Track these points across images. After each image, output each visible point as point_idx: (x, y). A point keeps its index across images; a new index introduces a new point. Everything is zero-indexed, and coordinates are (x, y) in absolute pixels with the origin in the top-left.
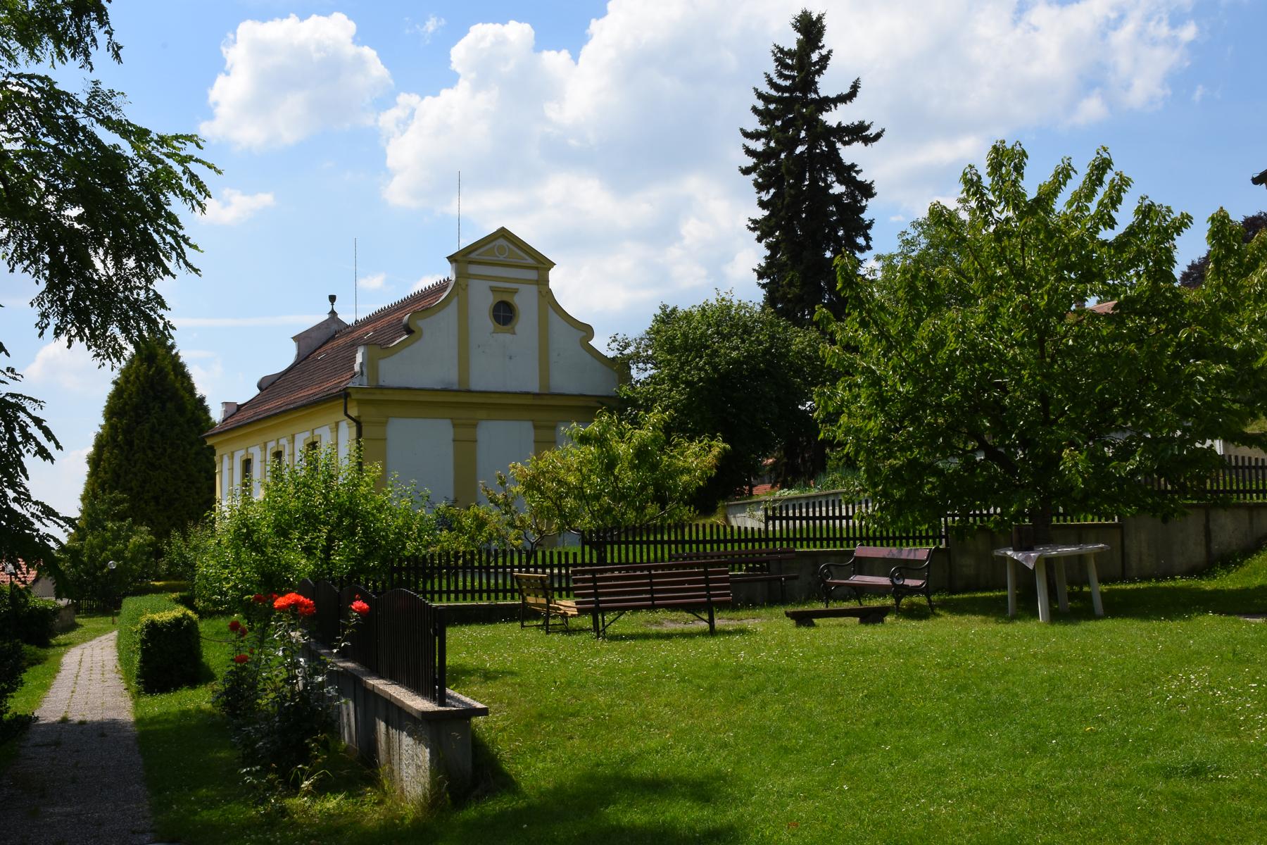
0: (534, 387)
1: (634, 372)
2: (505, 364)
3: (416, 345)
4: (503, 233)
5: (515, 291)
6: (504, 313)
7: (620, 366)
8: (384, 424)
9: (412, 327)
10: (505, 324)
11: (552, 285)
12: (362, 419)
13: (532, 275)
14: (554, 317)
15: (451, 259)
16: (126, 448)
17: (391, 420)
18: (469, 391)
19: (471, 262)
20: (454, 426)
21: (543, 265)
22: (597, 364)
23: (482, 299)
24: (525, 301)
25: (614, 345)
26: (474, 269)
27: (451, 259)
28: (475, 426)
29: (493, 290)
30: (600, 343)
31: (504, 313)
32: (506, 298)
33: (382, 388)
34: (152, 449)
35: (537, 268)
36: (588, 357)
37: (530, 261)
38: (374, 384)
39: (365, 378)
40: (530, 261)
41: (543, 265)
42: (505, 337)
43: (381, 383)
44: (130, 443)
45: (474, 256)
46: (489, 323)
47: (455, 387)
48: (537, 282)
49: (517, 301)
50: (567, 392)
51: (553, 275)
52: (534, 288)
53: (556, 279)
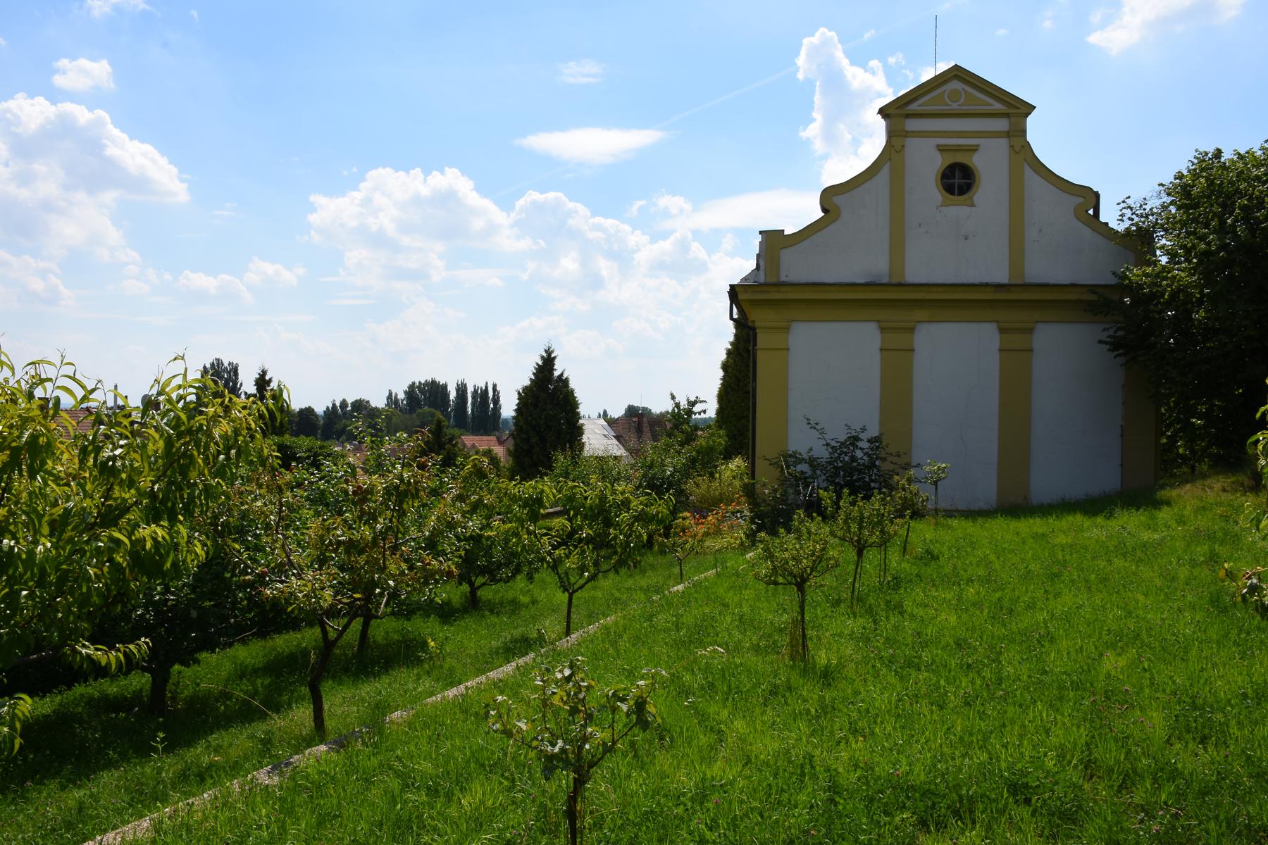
0: (1001, 275)
3: (832, 228)
4: (957, 74)
5: (974, 149)
6: (958, 180)
7: (1139, 240)
8: (786, 329)
11: (1030, 137)
13: (1001, 125)
14: (1033, 181)
15: (883, 112)
17: (794, 325)
19: (909, 116)
20: (883, 330)
21: (1018, 110)
23: (926, 162)
24: (990, 162)
26: (912, 125)
27: (883, 112)
28: (912, 330)
29: (942, 149)
31: (958, 180)
32: (960, 158)
33: (780, 285)
35: (1007, 115)
36: (1087, 232)
37: (998, 107)
38: (773, 280)
39: (762, 273)
40: (998, 107)
41: (1018, 110)
42: (957, 211)
43: (783, 278)
45: (914, 107)
46: (935, 194)
47: (885, 280)
48: (1008, 135)
49: (976, 162)
50: (1052, 281)
51: (1031, 120)
52: (1003, 143)
53: (1038, 133)
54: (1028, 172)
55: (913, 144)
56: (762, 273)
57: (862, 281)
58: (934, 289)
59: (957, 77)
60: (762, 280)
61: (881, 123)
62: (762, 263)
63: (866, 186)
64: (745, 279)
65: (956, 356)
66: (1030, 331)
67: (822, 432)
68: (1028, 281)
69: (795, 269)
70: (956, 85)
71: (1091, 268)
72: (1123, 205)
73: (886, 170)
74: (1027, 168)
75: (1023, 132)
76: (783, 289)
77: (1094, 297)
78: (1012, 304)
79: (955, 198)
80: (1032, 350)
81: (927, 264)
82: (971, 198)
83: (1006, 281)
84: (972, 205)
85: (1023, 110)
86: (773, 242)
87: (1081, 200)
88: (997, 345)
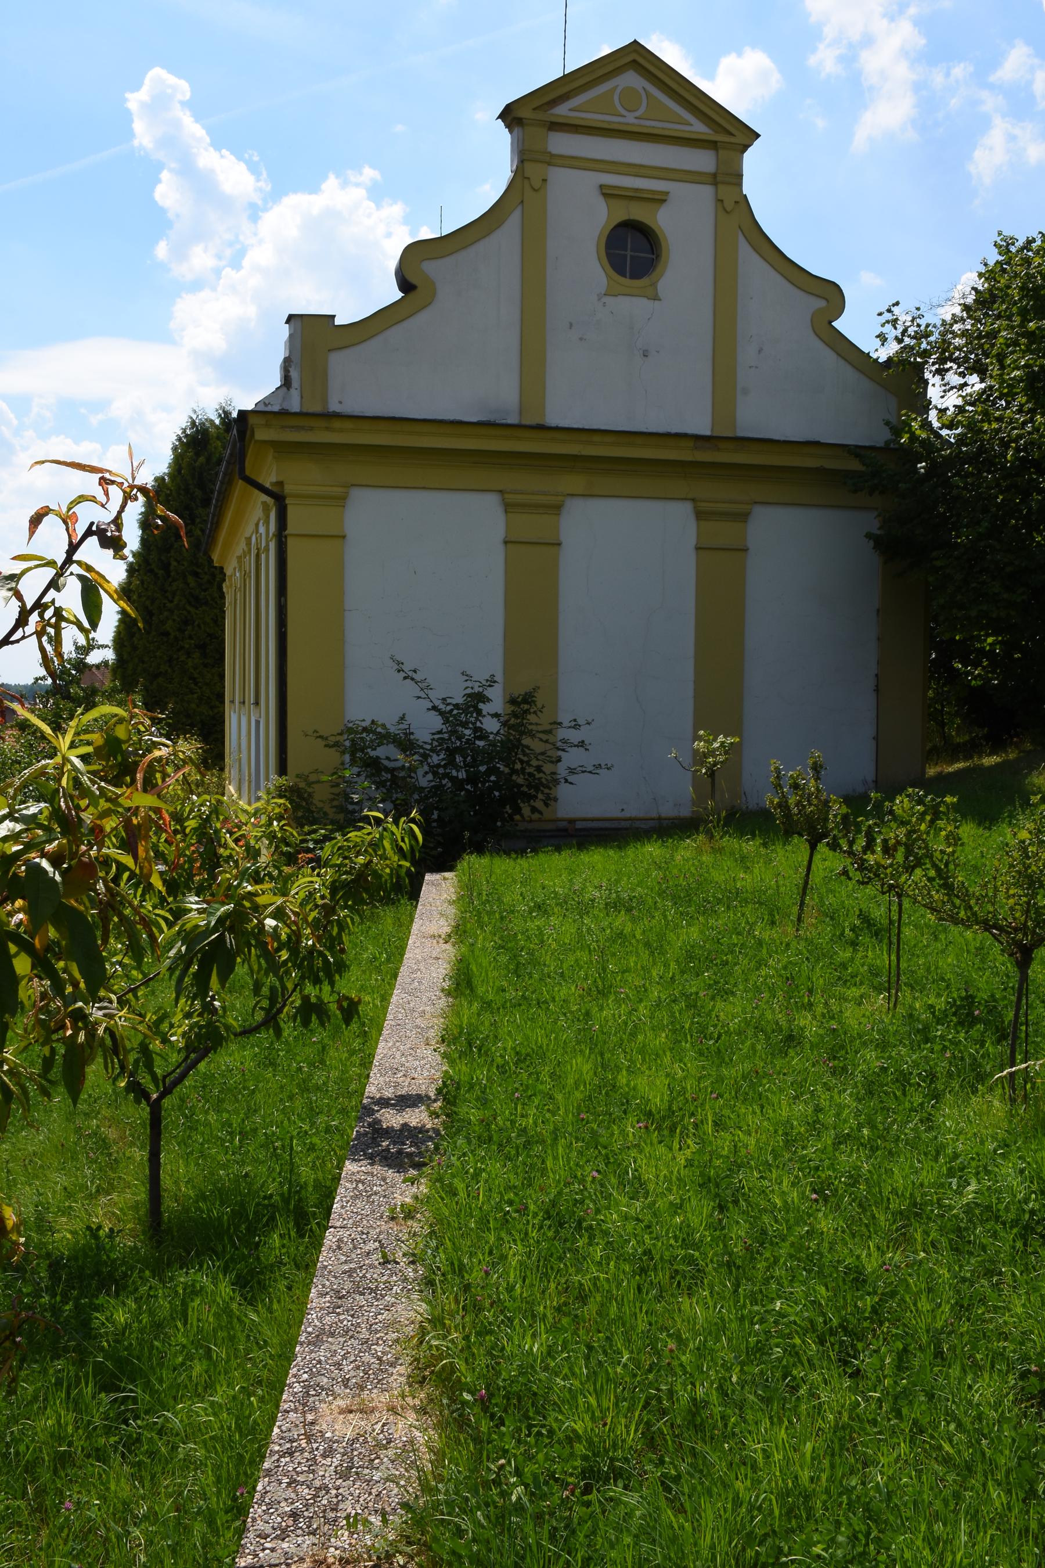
1: (934, 393)
2: (632, 367)
4: (635, 58)
5: (659, 199)
6: (634, 249)
7: (901, 378)
8: (341, 500)
9: (412, 279)
10: (636, 275)
11: (748, 188)
12: (288, 489)
13: (703, 161)
15: (510, 116)
16: (161, 572)
18: (542, 428)
19: (556, 126)
20: (508, 507)
22: (849, 374)
23: (580, 214)
24: (684, 222)
25: (891, 332)
26: (561, 144)
27: (510, 116)
28: (557, 509)
29: (608, 193)
30: (860, 326)
31: (634, 249)
32: (638, 213)
34: (196, 574)
37: (698, 128)
38: (317, 408)
39: (295, 393)
40: (698, 128)
42: (632, 307)
43: (334, 407)
44: (166, 567)
45: (562, 111)
46: (594, 271)
47: (513, 420)
48: (714, 179)
49: (663, 221)
51: (751, 160)
52: (706, 192)
54: (744, 248)
55: (560, 178)
56: (295, 393)
57: (474, 419)
58: (597, 438)
59: (635, 65)
60: (295, 406)
61: (502, 139)
62: (294, 374)
63: (481, 247)
64: (264, 402)
65: (626, 557)
66: (743, 517)
67: (425, 687)
68: (740, 433)
69: (357, 388)
70: (631, 80)
71: (844, 419)
72: (888, 316)
73: (514, 221)
74: (741, 238)
75: (737, 178)
76: (337, 424)
77: (855, 465)
78: (715, 469)
79: (627, 281)
80: (746, 550)
81: (586, 396)
82: (654, 285)
83: (708, 432)
84: (656, 298)
85: (739, 139)
86: (312, 337)
87: (822, 303)
88: (692, 541)
